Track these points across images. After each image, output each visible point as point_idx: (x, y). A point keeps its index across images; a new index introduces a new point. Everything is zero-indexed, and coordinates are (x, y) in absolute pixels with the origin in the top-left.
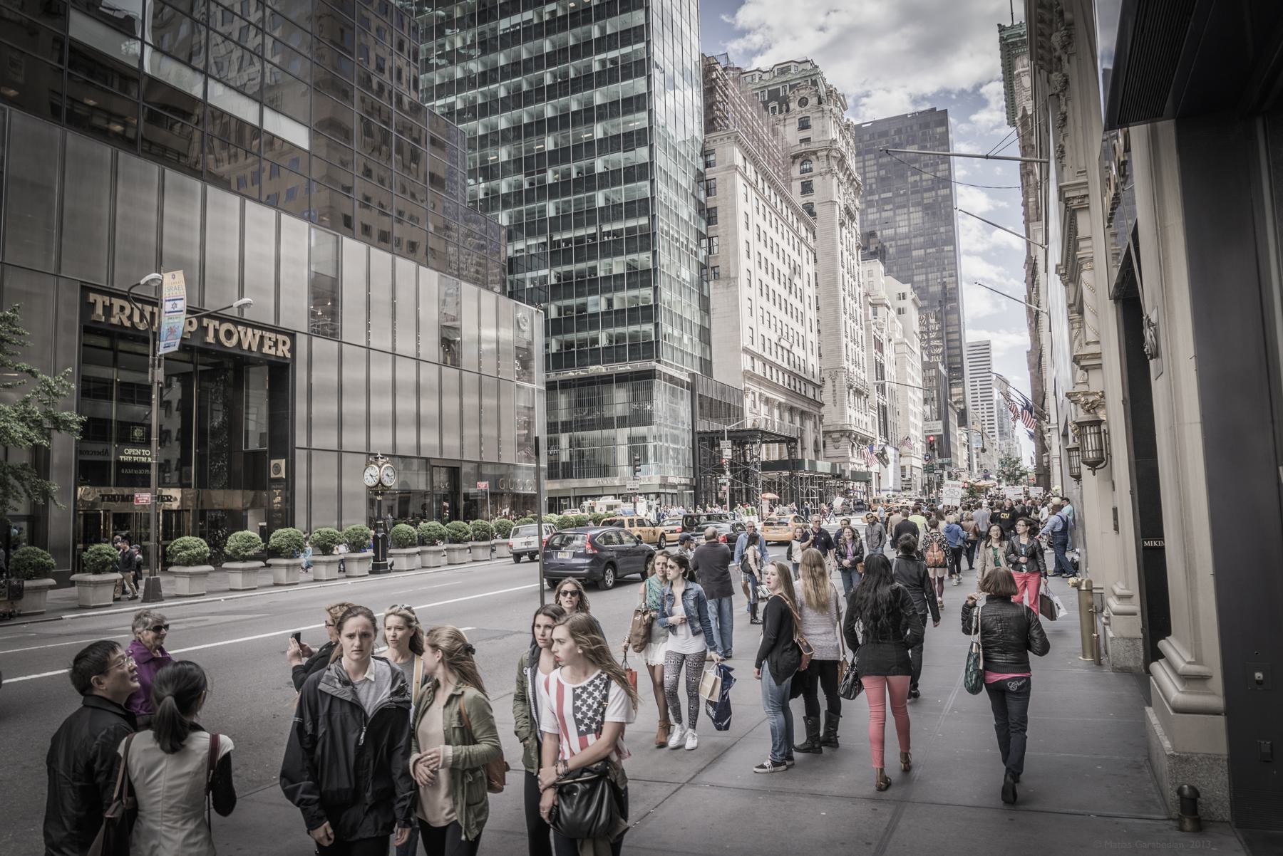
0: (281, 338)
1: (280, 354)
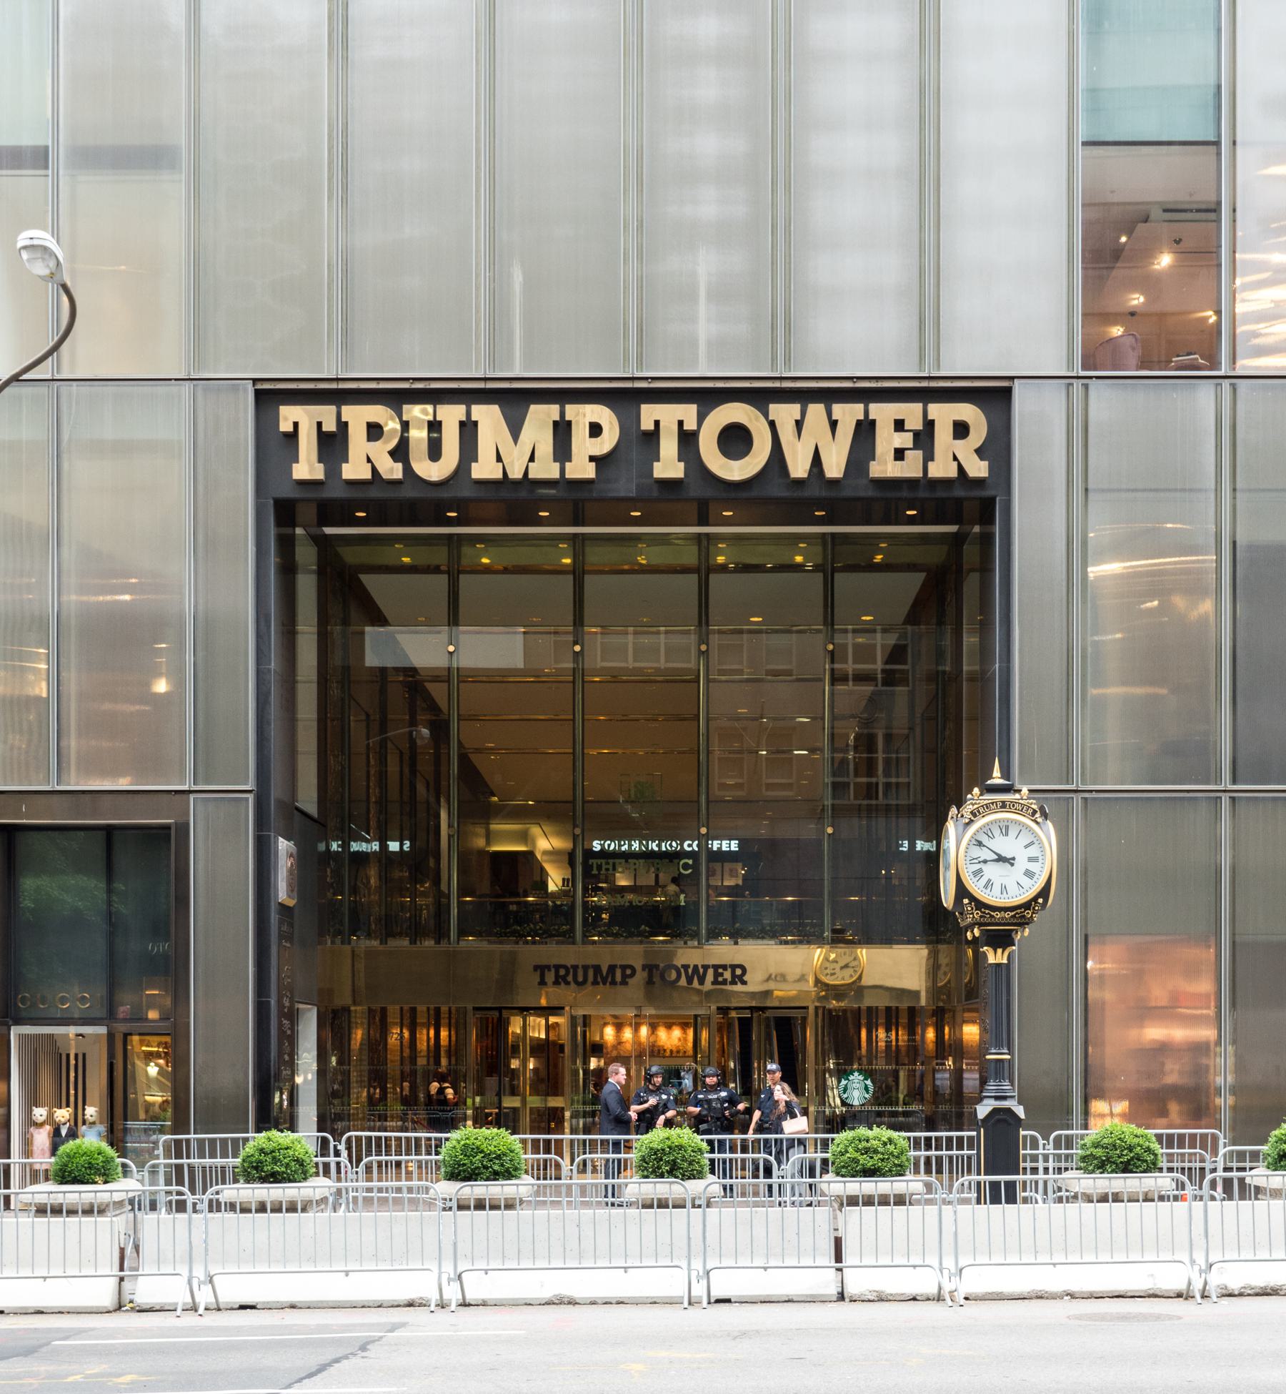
1: (941, 469)
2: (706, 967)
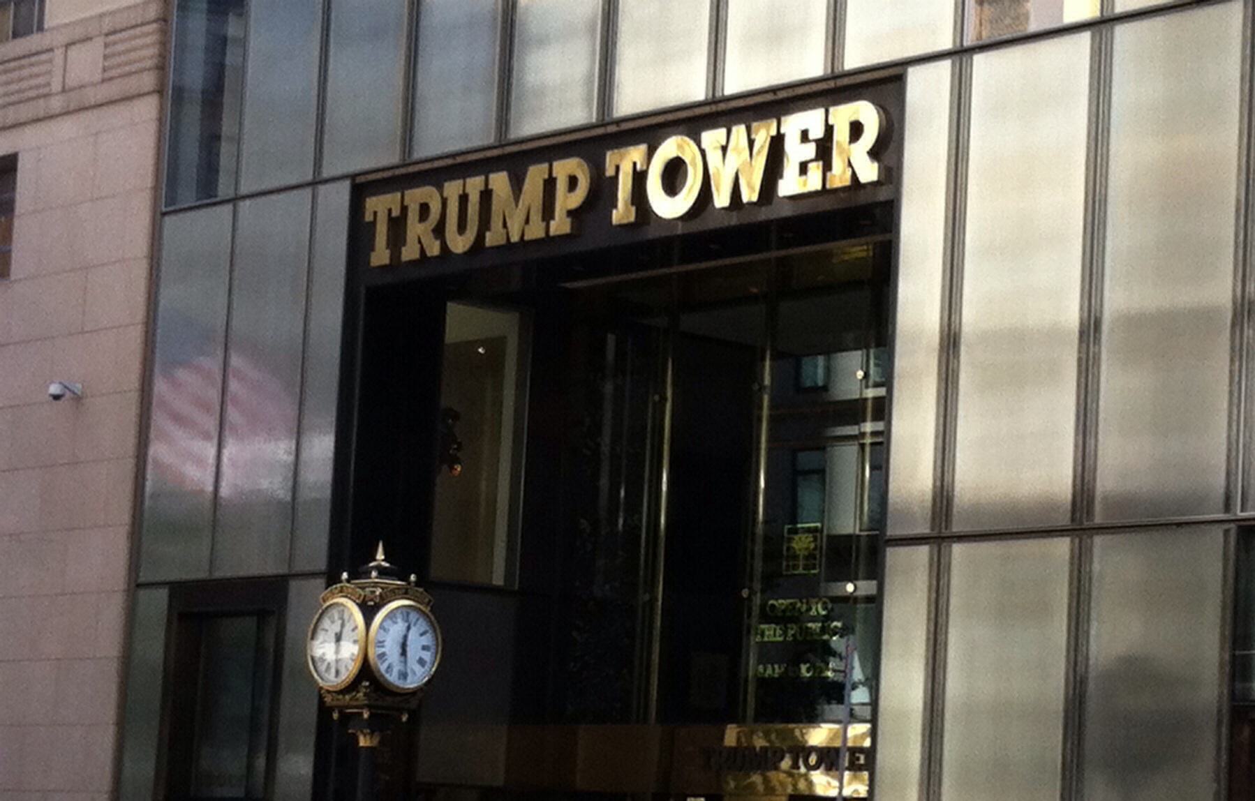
0: (842, 115)
1: (839, 177)
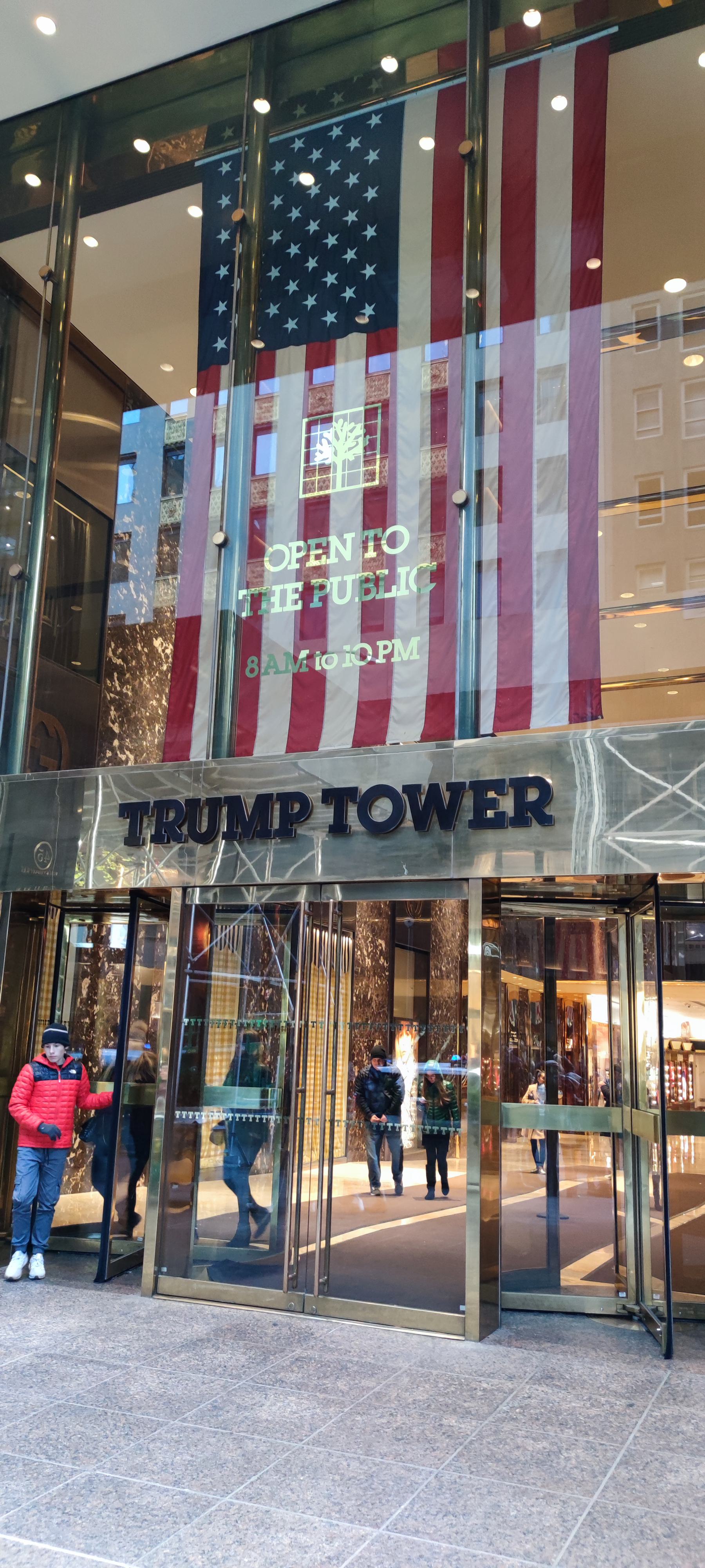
2: (456, 789)
